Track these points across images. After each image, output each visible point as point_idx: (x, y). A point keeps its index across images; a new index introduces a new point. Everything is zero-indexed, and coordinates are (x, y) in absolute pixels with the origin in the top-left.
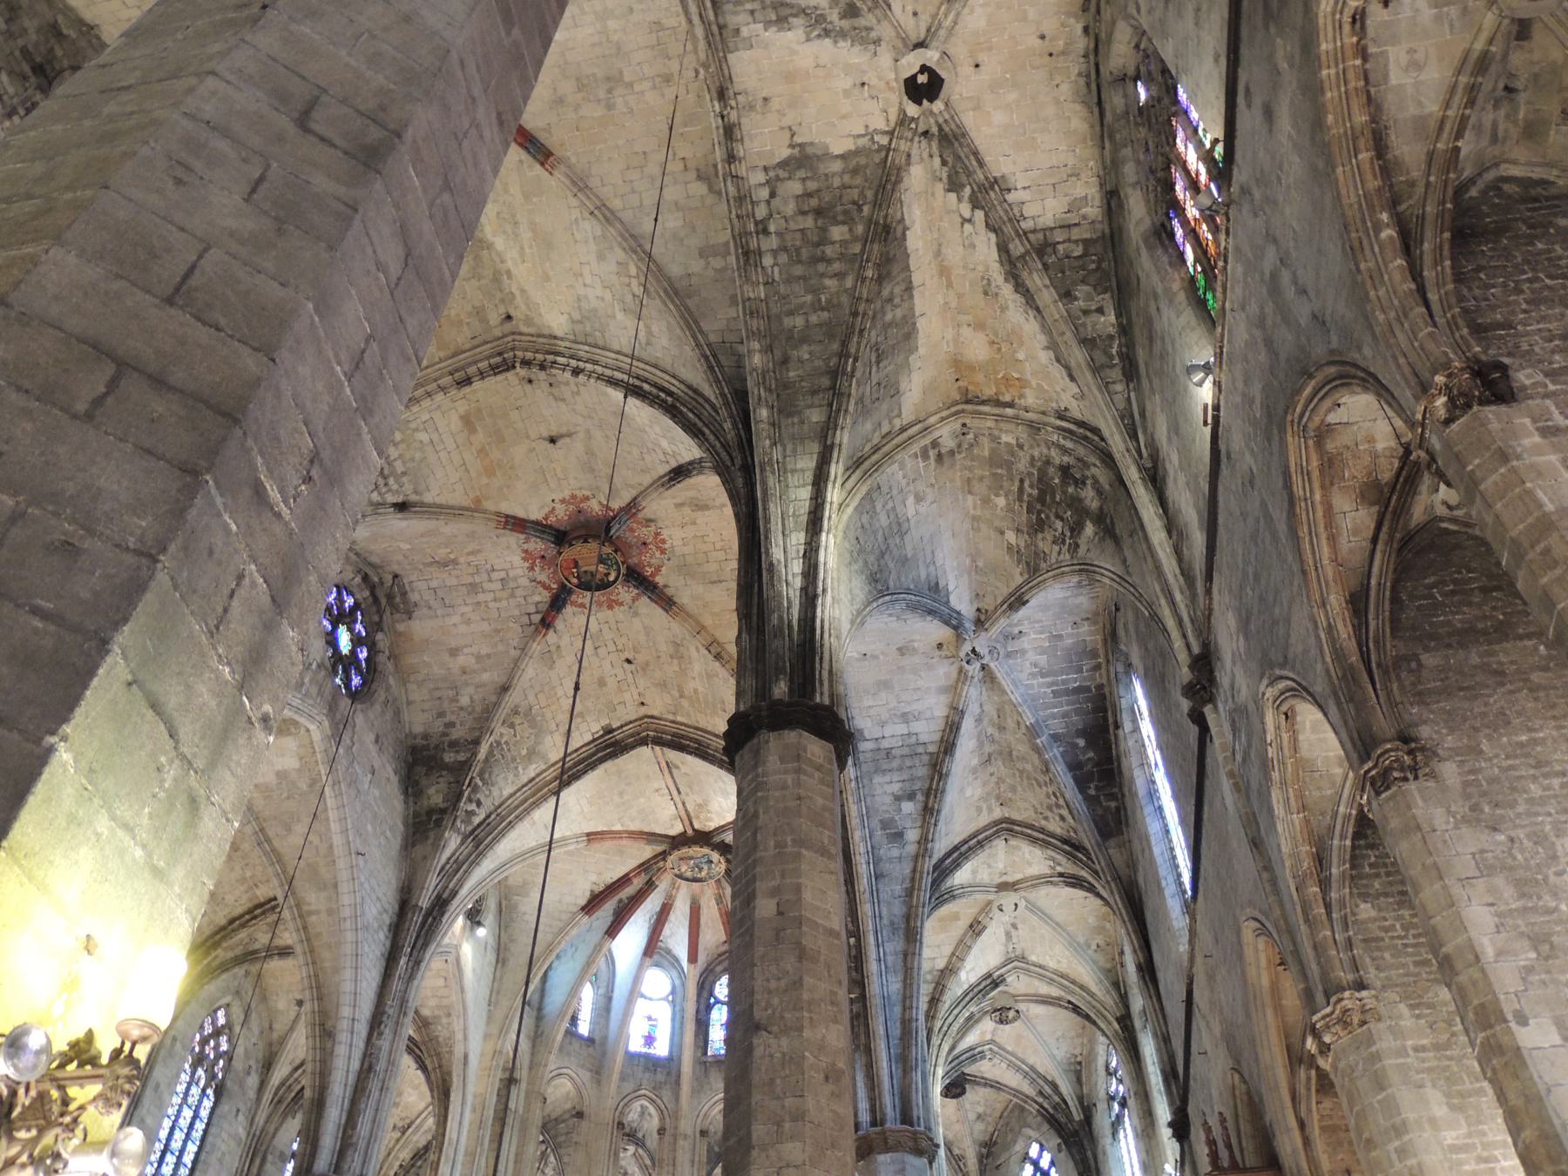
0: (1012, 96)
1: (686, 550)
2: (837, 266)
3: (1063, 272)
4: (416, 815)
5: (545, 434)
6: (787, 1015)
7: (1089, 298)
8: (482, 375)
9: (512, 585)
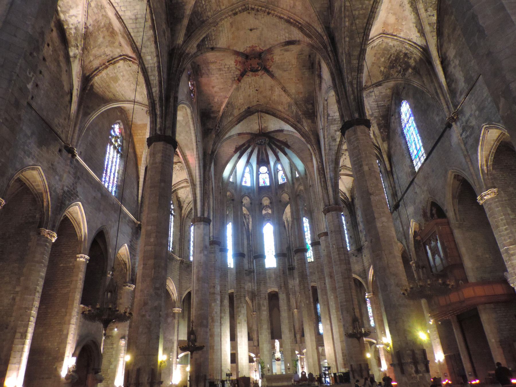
1: (279, 62)
3: (426, 4)
5: (249, 28)
6: (377, 192)
7: (431, 12)
8: (240, 11)
9: (230, 69)
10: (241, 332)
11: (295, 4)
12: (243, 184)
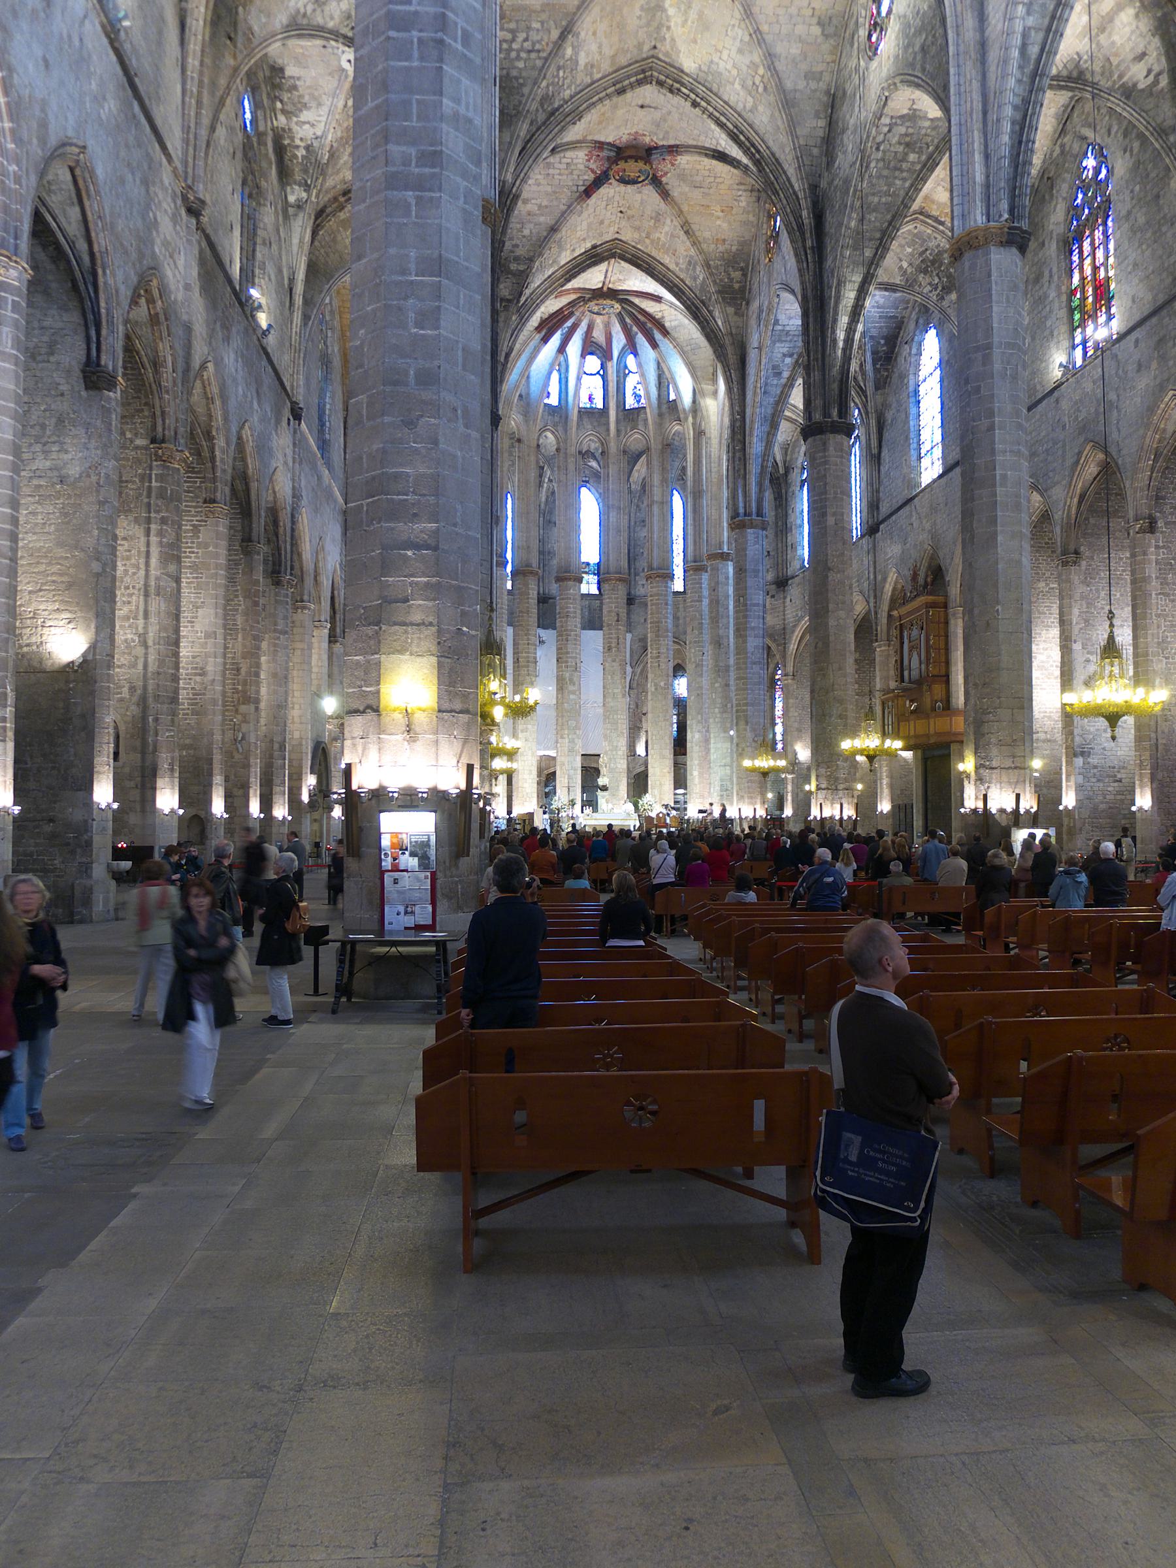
2: (905, 174)
8: (632, 86)
12: (546, 401)
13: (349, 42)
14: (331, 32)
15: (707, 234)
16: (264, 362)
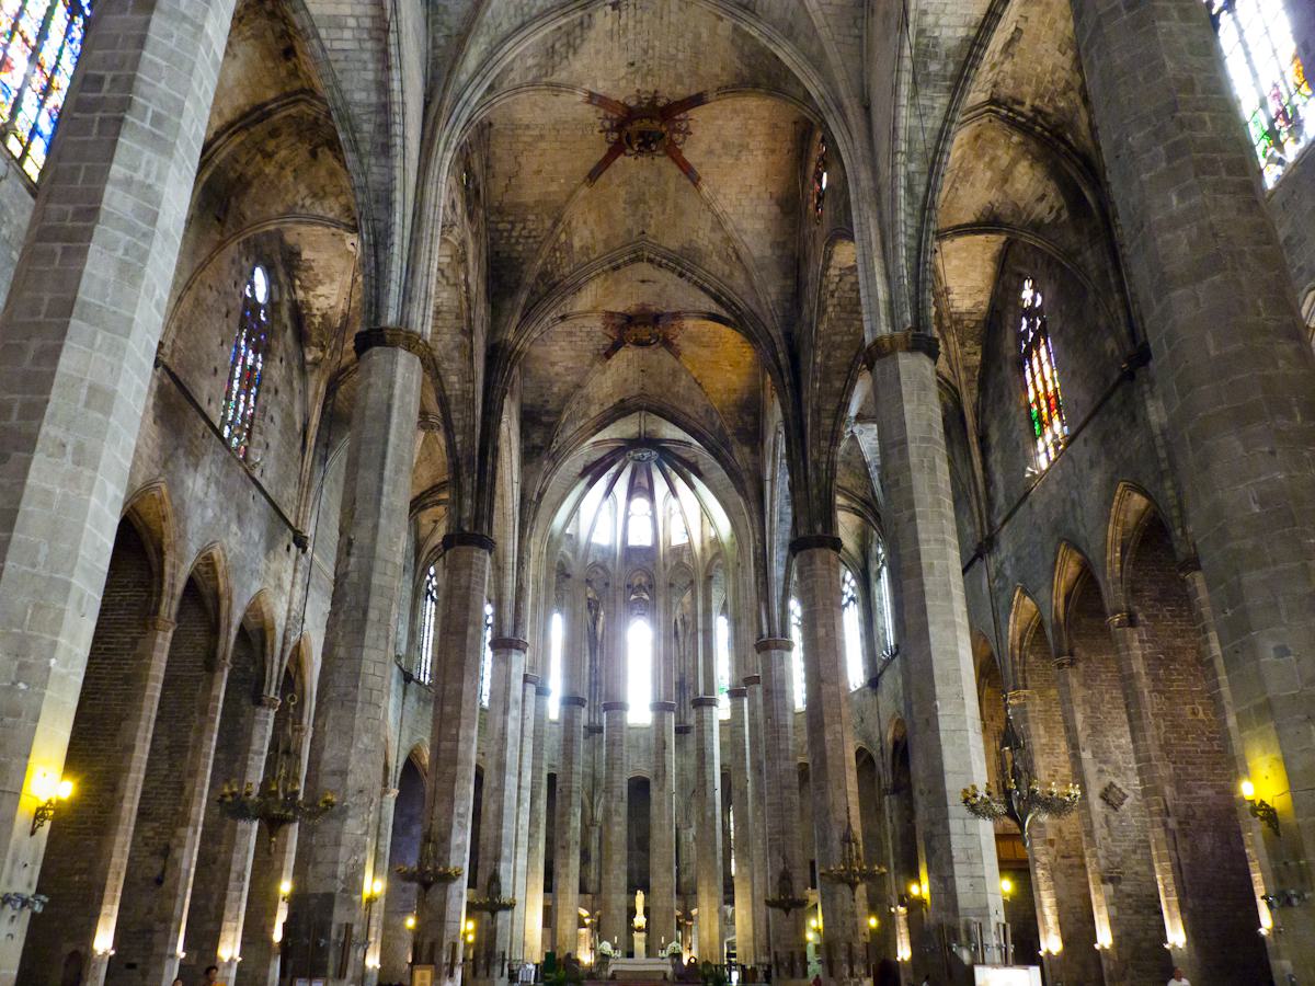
0: (964, 255)
4: (526, 447)
8: (625, 264)
10: (566, 865)
11: (732, 273)
13: (355, 229)
14: (332, 221)
15: (719, 386)
16: (254, 491)
